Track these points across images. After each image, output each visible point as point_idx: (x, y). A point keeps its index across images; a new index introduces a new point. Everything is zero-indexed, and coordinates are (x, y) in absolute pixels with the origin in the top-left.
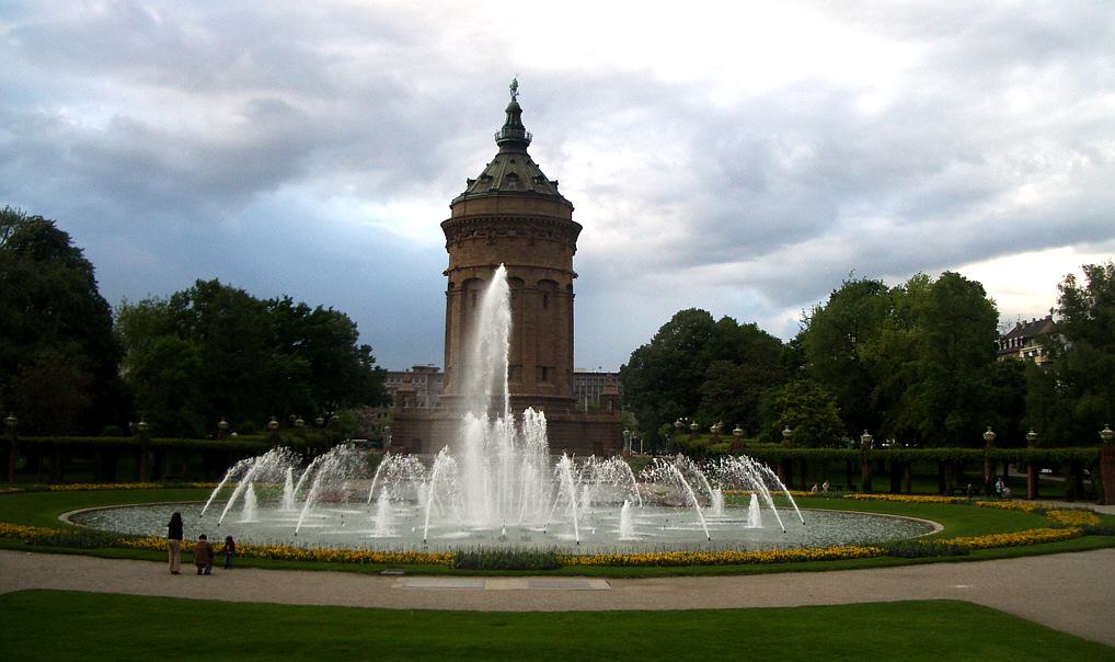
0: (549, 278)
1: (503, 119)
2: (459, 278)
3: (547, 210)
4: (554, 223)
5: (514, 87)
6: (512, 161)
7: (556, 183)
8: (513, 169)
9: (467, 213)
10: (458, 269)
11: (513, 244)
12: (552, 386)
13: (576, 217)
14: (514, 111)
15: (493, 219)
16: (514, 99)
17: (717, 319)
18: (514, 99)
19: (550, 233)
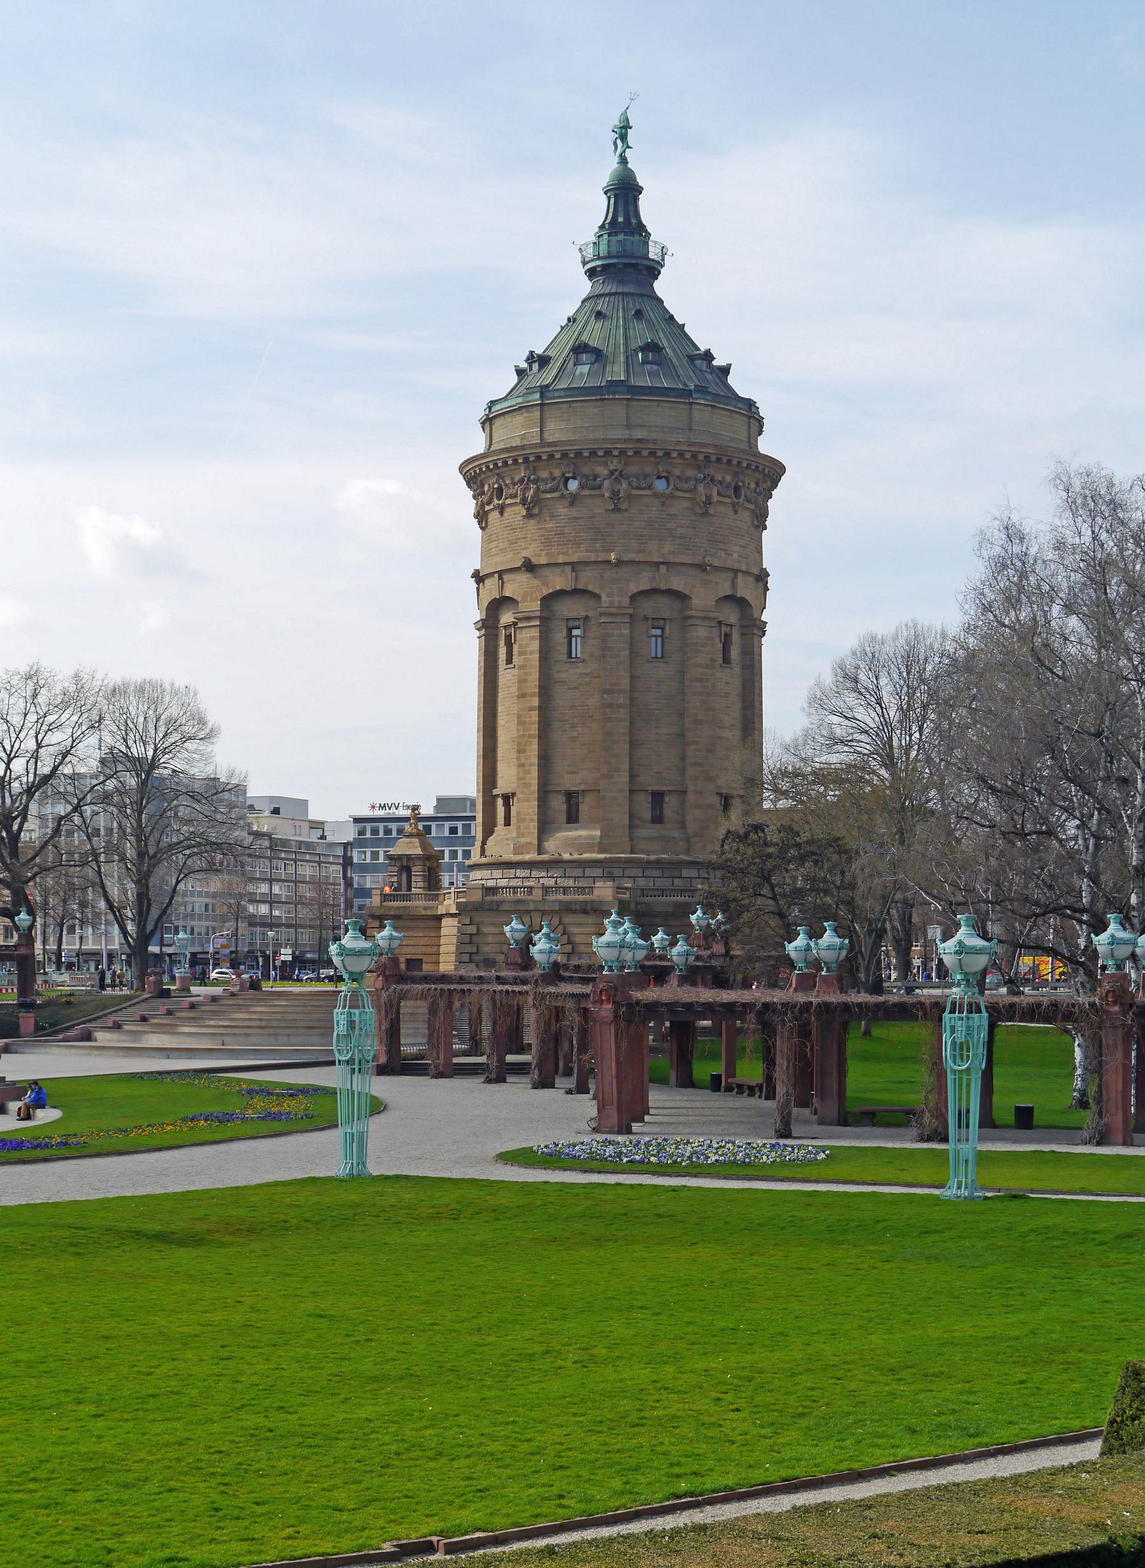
0: (663, 587)
3: (661, 423)
4: (667, 454)
5: (623, 131)
8: (595, 335)
12: (676, 834)
14: (625, 191)
16: (623, 161)
18: (623, 161)
19: (667, 478)
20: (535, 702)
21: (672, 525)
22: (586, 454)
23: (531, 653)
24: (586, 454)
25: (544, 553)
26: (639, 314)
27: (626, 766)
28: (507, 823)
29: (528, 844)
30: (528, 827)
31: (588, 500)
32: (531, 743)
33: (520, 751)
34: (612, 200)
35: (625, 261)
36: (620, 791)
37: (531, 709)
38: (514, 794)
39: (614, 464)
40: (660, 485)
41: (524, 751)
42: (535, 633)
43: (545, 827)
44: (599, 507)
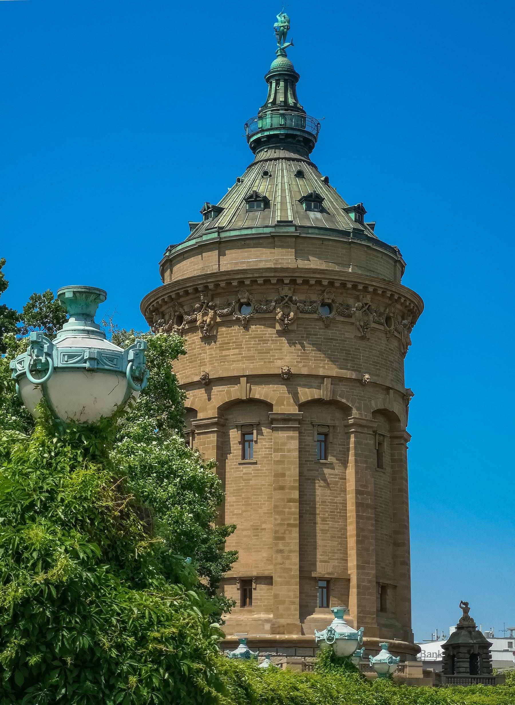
6: (300, 174)
8: (305, 188)
11: (329, 332)
20: (296, 494)
21: (391, 358)
22: (349, 285)
23: (289, 451)
24: (349, 285)
25: (300, 365)
27: (373, 559)
29: (288, 624)
30: (288, 609)
31: (340, 326)
32: (290, 532)
33: (277, 538)
34: (282, 84)
36: (370, 581)
37: (290, 500)
39: (368, 299)
41: (283, 538)
42: (296, 434)
43: (305, 611)
44: (350, 334)
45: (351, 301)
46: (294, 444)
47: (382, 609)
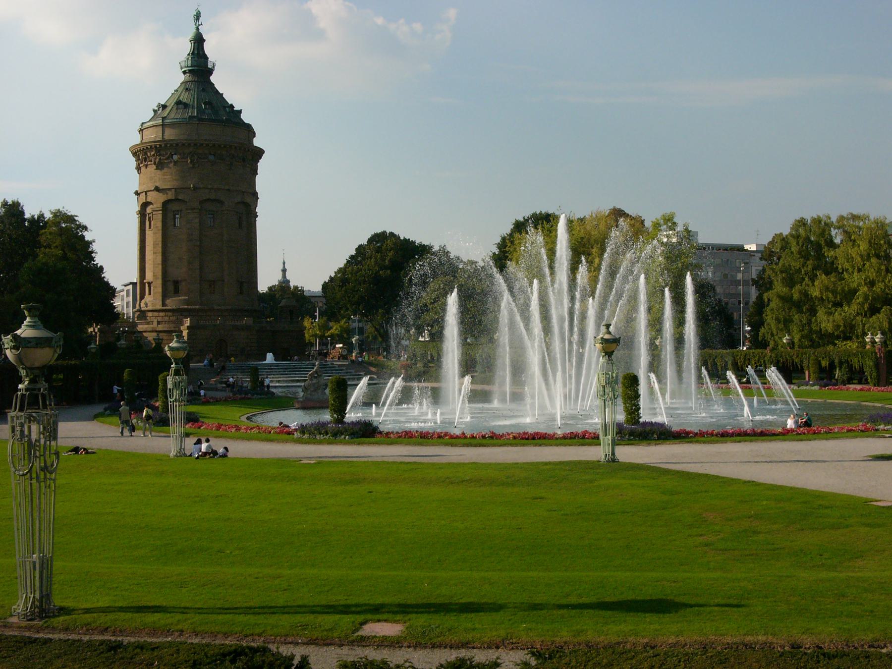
1: (187, 47)
2: (158, 200)
5: (198, 16)
7: (240, 112)
9: (166, 138)
10: (157, 189)
13: (257, 142)
14: (199, 41)
15: (214, 145)
16: (198, 29)
17: (402, 238)
18: (198, 29)
20: (198, 243)
26: (203, 90)
28: (150, 294)
35: (199, 68)
38: (185, 280)
40: (211, 158)
45: (224, 152)
46: (197, 220)
47: (241, 293)
